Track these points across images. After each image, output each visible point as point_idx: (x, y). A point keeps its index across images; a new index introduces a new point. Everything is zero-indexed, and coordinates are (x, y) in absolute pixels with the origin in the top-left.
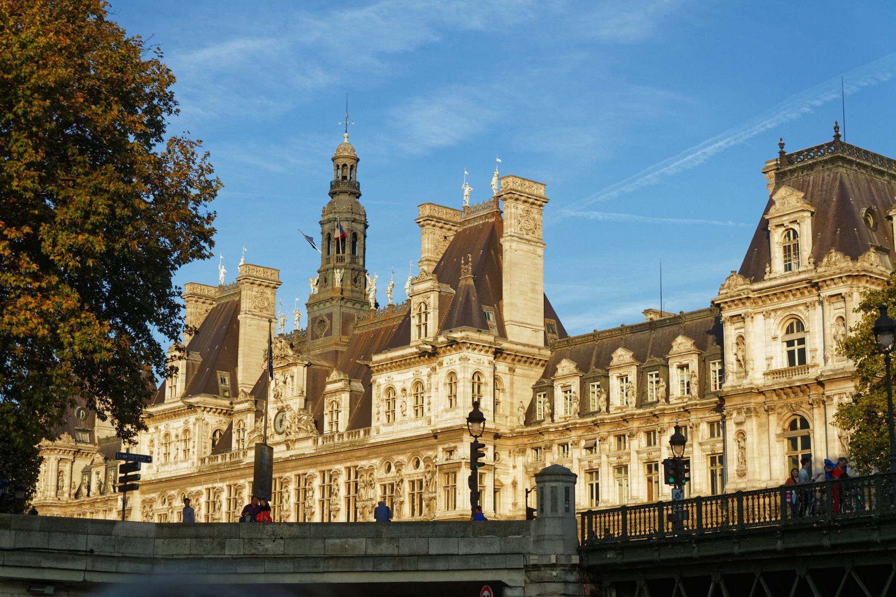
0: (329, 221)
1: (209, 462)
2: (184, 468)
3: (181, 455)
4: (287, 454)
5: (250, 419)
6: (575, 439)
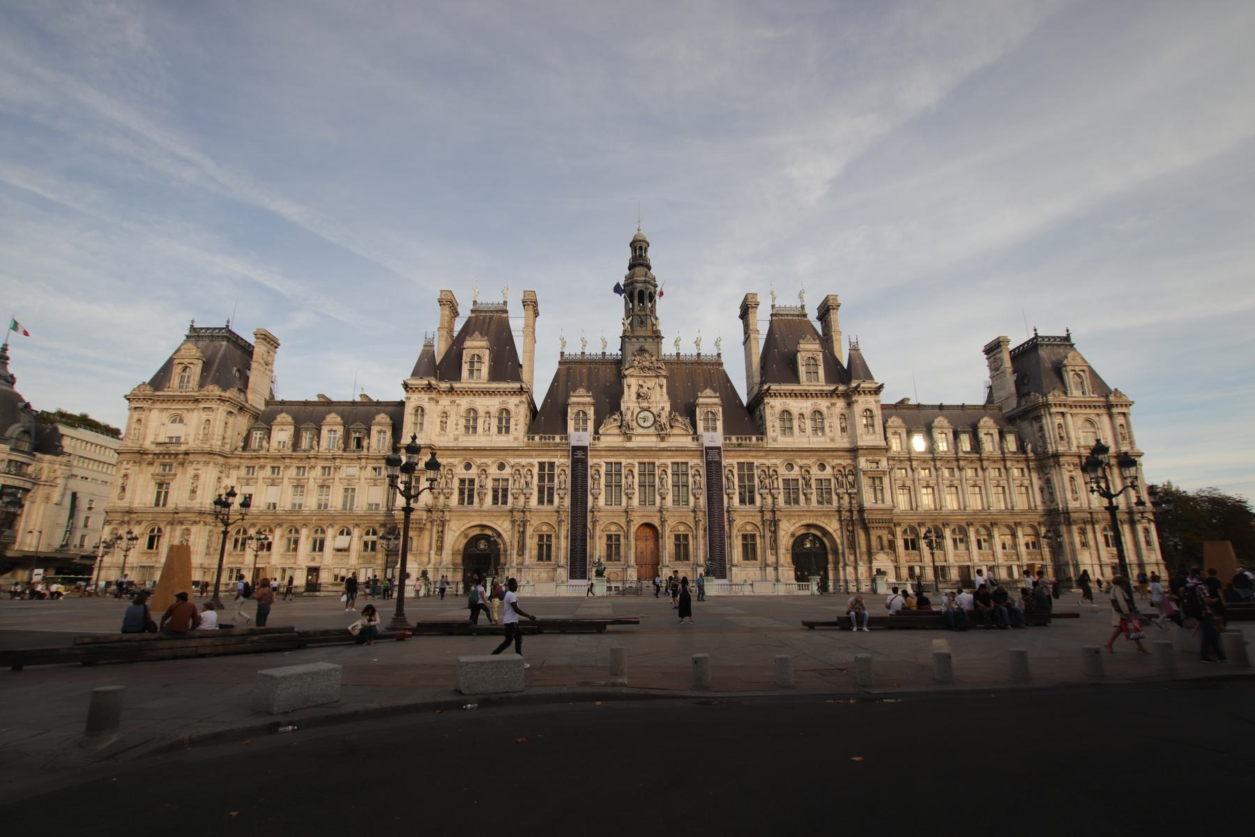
0: (645, 282)
1: (541, 439)
2: (504, 441)
3: (494, 429)
4: (663, 445)
5: (591, 412)
6: (916, 466)
